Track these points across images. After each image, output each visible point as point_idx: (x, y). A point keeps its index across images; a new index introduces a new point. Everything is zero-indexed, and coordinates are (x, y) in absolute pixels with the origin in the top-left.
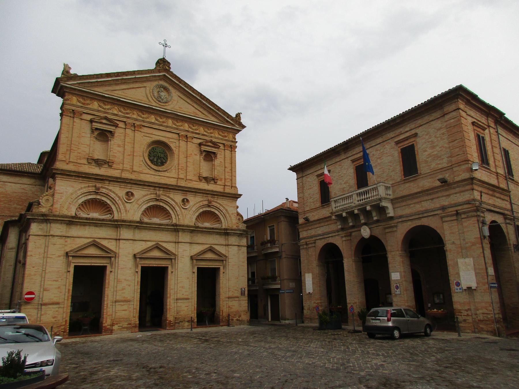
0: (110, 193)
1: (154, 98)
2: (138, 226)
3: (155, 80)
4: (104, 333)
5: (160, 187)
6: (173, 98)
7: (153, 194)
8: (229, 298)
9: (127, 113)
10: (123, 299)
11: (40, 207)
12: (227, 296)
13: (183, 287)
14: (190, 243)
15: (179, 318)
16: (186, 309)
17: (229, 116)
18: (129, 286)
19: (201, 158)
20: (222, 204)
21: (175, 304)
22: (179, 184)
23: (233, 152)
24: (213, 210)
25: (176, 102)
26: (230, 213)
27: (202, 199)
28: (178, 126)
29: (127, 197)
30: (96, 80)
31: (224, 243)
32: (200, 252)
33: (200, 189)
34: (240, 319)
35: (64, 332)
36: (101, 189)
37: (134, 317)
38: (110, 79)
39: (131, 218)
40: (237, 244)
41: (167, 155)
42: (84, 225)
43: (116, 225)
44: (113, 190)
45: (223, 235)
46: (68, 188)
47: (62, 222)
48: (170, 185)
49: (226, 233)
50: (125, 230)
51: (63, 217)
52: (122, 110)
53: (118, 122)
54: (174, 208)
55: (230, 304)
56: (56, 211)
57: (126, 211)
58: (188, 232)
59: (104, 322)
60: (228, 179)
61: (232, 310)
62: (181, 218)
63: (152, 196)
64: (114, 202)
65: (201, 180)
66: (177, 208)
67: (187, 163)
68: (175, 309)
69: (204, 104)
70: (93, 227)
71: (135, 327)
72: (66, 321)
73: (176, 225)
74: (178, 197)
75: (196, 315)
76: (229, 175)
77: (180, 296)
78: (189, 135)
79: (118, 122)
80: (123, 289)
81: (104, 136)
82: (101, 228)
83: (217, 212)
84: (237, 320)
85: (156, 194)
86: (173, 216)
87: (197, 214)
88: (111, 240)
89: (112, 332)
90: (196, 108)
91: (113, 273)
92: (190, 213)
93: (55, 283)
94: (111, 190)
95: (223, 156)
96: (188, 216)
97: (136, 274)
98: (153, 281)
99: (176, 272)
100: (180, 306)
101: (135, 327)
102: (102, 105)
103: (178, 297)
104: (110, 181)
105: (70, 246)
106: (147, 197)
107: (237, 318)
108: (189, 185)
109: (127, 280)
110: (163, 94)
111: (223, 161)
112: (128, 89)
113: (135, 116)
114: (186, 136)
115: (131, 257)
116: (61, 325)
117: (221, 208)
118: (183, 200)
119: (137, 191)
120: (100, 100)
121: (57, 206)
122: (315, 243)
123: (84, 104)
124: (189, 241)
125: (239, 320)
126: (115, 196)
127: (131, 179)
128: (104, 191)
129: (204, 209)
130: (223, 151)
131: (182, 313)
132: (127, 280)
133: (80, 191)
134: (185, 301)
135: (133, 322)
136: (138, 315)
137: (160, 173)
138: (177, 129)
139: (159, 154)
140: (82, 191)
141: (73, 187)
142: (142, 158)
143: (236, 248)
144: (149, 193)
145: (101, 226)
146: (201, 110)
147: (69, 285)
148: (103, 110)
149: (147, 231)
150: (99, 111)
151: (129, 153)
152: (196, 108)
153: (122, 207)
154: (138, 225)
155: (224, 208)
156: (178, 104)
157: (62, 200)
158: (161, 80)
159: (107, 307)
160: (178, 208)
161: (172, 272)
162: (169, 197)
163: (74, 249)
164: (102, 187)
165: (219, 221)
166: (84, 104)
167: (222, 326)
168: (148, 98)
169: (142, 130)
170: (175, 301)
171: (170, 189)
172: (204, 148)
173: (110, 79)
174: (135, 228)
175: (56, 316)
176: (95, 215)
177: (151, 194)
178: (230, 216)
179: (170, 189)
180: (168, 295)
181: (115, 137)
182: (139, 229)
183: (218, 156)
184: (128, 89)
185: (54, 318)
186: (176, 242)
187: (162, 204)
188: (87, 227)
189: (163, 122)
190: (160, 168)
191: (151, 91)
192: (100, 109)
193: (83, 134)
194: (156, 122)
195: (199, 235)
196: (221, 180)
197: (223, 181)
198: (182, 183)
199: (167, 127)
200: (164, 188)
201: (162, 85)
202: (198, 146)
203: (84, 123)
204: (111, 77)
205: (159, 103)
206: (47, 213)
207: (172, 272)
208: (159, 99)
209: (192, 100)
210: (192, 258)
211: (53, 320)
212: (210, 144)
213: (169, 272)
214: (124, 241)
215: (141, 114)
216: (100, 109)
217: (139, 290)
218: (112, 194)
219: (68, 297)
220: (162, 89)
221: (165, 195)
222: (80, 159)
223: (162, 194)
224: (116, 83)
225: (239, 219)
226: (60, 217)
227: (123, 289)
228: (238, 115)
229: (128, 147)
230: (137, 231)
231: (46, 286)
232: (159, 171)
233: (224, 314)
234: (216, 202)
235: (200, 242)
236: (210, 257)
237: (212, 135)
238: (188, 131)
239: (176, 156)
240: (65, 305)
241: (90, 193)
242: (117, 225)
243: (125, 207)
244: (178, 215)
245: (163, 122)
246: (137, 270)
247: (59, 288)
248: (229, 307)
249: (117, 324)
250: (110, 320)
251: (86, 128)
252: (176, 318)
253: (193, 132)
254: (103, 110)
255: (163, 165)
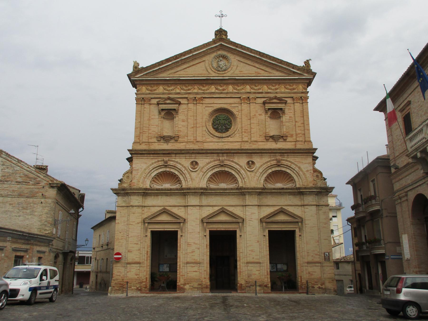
0: (177, 164)
1: (213, 69)
2: (203, 192)
3: (214, 52)
4: (178, 291)
5: (223, 153)
6: (232, 64)
7: (217, 160)
8: (308, 263)
9: (189, 90)
10: (193, 261)
11: (123, 183)
12: (306, 261)
13: (252, 251)
14: (258, 206)
15: (250, 282)
16: (257, 273)
17: (294, 66)
18: (199, 249)
19: (267, 117)
20: (293, 161)
21: (246, 267)
22: (242, 148)
23: (304, 104)
24: (284, 169)
25: (235, 67)
26: (304, 170)
27: (270, 159)
28: (238, 90)
29: (192, 166)
30: (159, 67)
31: (300, 203)
32: (269, 215)
33: (264, 149)
34: (323, 287)
35: (145, 288)
36: (169, 162)
37: (205, 278)
38: (170, 63)
39: (197, 186)
40: (315, 203)
41: (231, 121)
42: (157, 195)
43: (183, 193)
44: (179, 161)
45: (298, 195)
46: (142, 165)
47: (138, 194)
48: (232, 149)
49: (300, 192)
50: (192, 197)
51: (138, 190)
52: (184, 88)
53: (179, 100)
54: (239, 171)
55: (310, 269)
56: (134, 185)
57: (192, 179)
58: (255, 194)
59: (178, 281)
60: (299, 134)
61: (313, 277)
62: (247, 181)
63: (216, 162)
64: (181, 172)
65: (267, 140)
66: (242, 172)
67: (252, 124)
68: (246, 272)
69: (265, 61)
70: (165, 197)
71: (207, 287)
72: (146, 278)
73: (241, 188)
74: (243, 161)
75: (269, 280)
76: (301, 130)
77: (250, 259)
78: (251, 96)
79: (179, 100)
80: (193, 252)
81: (169, 114)
82: (171, 197)
83: (288, 171)
84: (319, 288)
85: (220, 160)
86: (239, 180)
87: (265, 175)
88: (180, 207)
89: (184, 291)
90: (257, 68)
91: (183, 237)
92: (257, 175)
93: (135, 245)
94: (177, 162)
95: (292, 111)
96: (254, 179)
97: (205, 238)
98: (223, 245)
99: (245, 235)
100: (251, 270)
101: (207, 287)
102: (166, 87)
103: (248, 261)
104: (176, 154)
105: (147, 214)
106: (211, 164)
107: (319, 285)
108: (254, 147)
109: (196, 244)
110: (223, 63)
111: (292, 116)
112: (188, 67)
113: (196, 91)
114: (248, 97)
115: (198, 222)
116: (143, 282)
117: (293, 166)
118: (248, 163)
119: (201, 159)
120: (164, 84)
121: (135, 181)
122: (406, 195)
123: (151, 91)
124: (256, 204)
125: (322, 288)
126: (181, 166)
127: (194, 150)
128: (171, 163)
129: (274, 169)
130: (292, 105)
131: (253, 277)
132: (196, 244)
133: (152, 166)
134: (256, 265)
135: (204, 283)
136: (208, 276)
137: (223, 140)
138: (238, 93)
139: (223, 121)
140: (153, 166)
141: (146, 163)
142: (205, 128)
143: (314, 208)
144: (213, 159)
145: (171, 195)
146: (264, 68)
147: (148, 248)
148: (167, 92)
149: (213, 196)
150: (163, 94)
151: (192, 126)
152: (257, 68)
153: (188, 176)
154: (203, 191)
155: (296, 165)
156: (239, 68)
157: (138, 176)
158: (219, 50)
159: (180, 267)
160: (243, 171)
161: (241, 236)
162: (232, 161)
163: (149, 217)
164: (169, 160)
165: (292, 180)
166: (151, 91)
167: (300, 293)
168: (207, 71)
169: (204, 102)
170: (246, 265)
171: (234, 153)
172: (268, 106)
173: (170, 63)
174: (201, 195)
175: (138, 273)
176: (167, 186)
177: (215, 161)
178: (304, 174)
179: (234, 153)
180: (238, 259)
181: (179, 113)
182: (205, 195)
183: (286, 111)
184: (188, 67)
185: (137, 275)
186: (243, 206)
187: (227, 169)
188: (160, 197)
189: (224, 90)
190: (224, 135)
191: (210, 63)
192: (165, 91)
193: (153, 117)
194: (217, 91)
195: (269, 197)
196: (292, 136)
197: (294, 137)
198: (246, 146)
199: (227, 93)
200: (227, 153)
201: (220, 55)
202: (262, 105)
203: (152, 107)
204: (171, 61)
205: (219, 72)
206: (128, 187)
207: (241, 236)
208: (218, 69)
209: (252, 61)
210: (261, 221)
211: (136, 277)
212: (275, 101)
213: (238, 236)
214: (192, 208)
215: (201, 87)
216: (165, 91)
217: (208, 254)
218: (179, 165)
219: (147, 258)
220: (221, 58)
221: (229, 160)
222: (151, 139)
223: (226, 160)
224: (177, 64)
225: (317, 176)
226: (135, 190)
227: (193, 252)
228: (307, 63)
229: (191, 121)
230: (204, 197)
231: (129, 248)
232: (222, 138)
233: (304, 281)
234: (287, 161)
235: (271, 204)
236: (283, 219)
237: (278, 91)
238: (250, 93)
239: (238, 120)
240: (145, 265)
241: (160, 167)
242: (184, 193)
243: (190, 175)
244: (244, 179)
245: (224, 90)
246: (205, 234)
247: (139, 250)
248: (309, 273)
249: (188, 284)
250: (183, 280)
251: (155, 110)
252: (246, 282)
253: (255, 93)
254: (167, 92)
255: (228, 131)
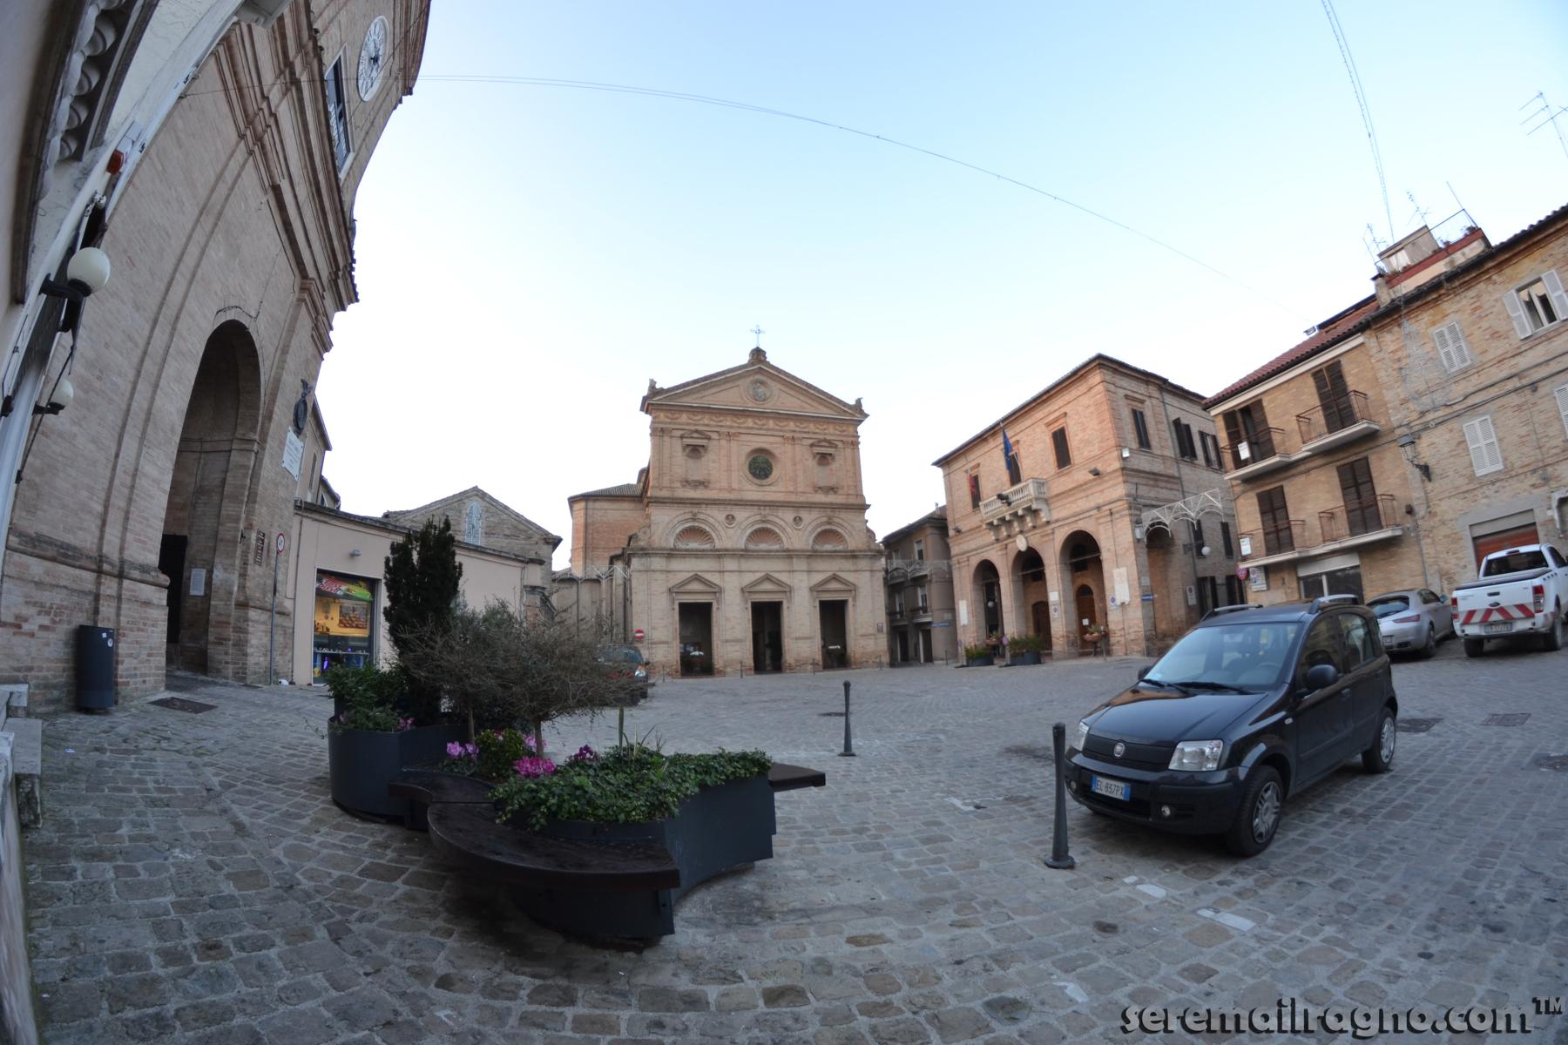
17: (845, 404)
49: (853, 556)
67: (795, 471)
74: (789, 515)
98: (767, 618)
108: (802, 499)
110: (761, 390)
115: (738, 592)
139: (760, 466)
190: (765, 482)
198: (793, 498)
208: (756, 398)
210: (812, 589)
224: (705, 388)
228: (859, 401)
241: (686, 520)
